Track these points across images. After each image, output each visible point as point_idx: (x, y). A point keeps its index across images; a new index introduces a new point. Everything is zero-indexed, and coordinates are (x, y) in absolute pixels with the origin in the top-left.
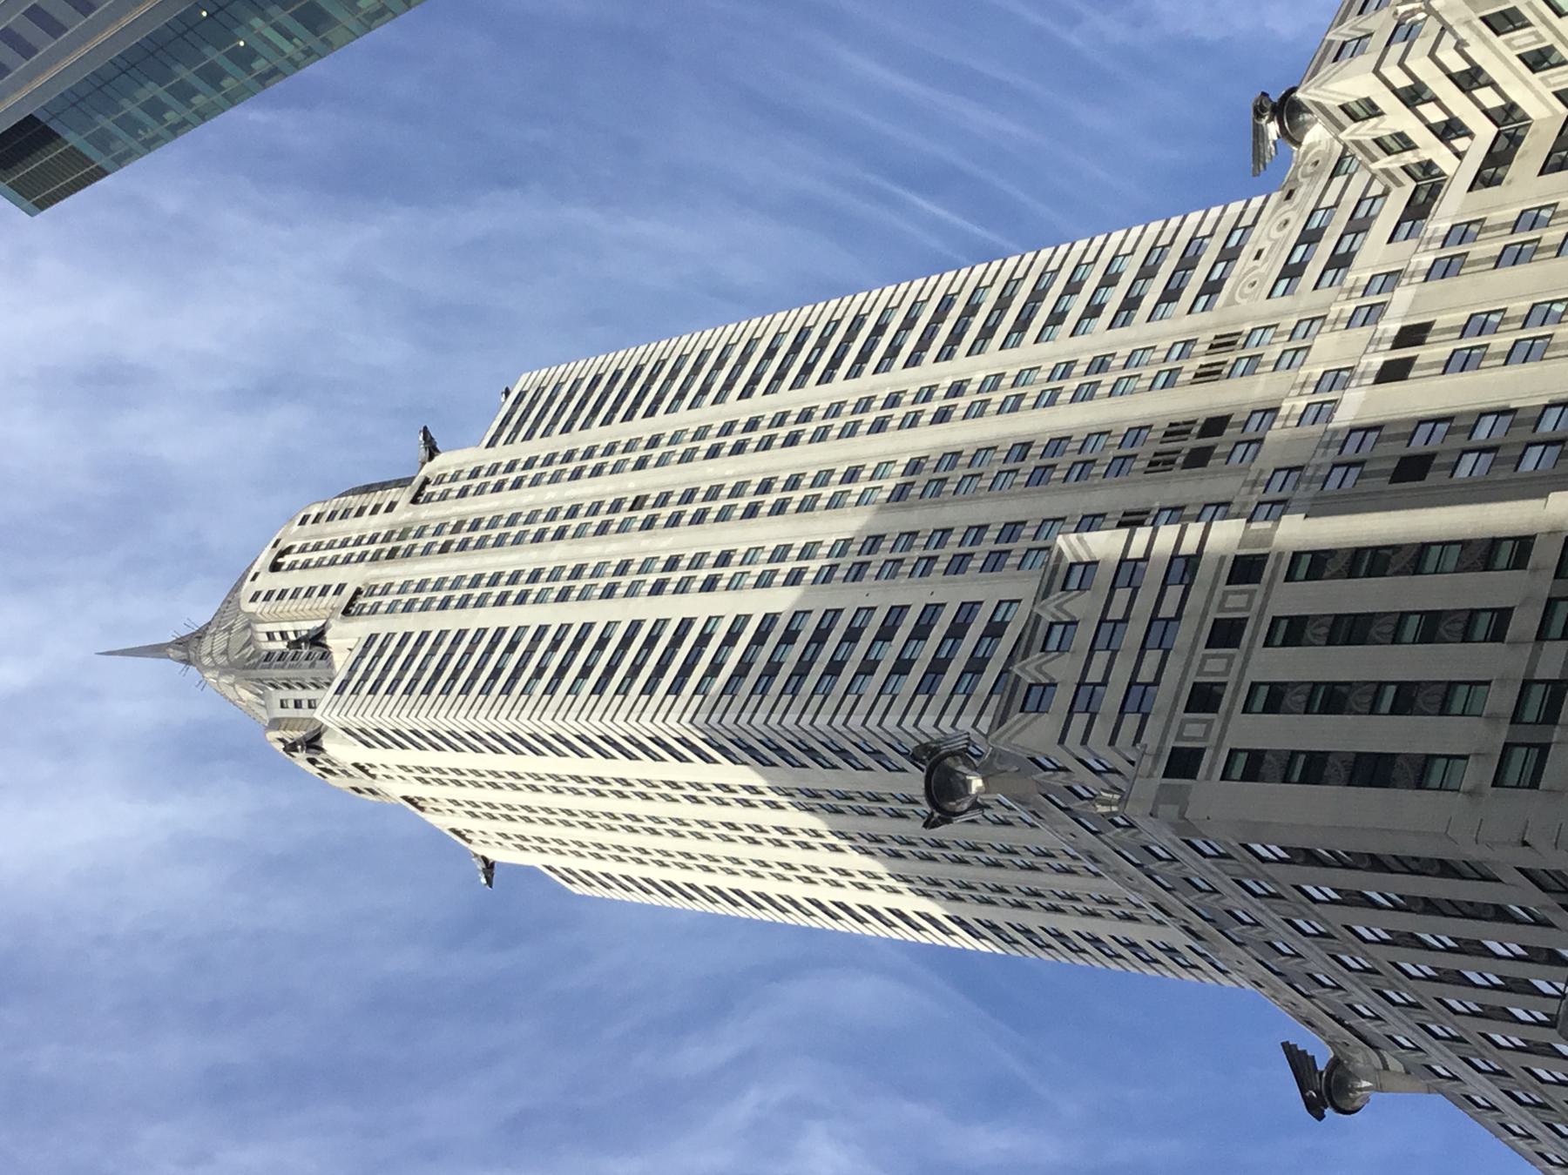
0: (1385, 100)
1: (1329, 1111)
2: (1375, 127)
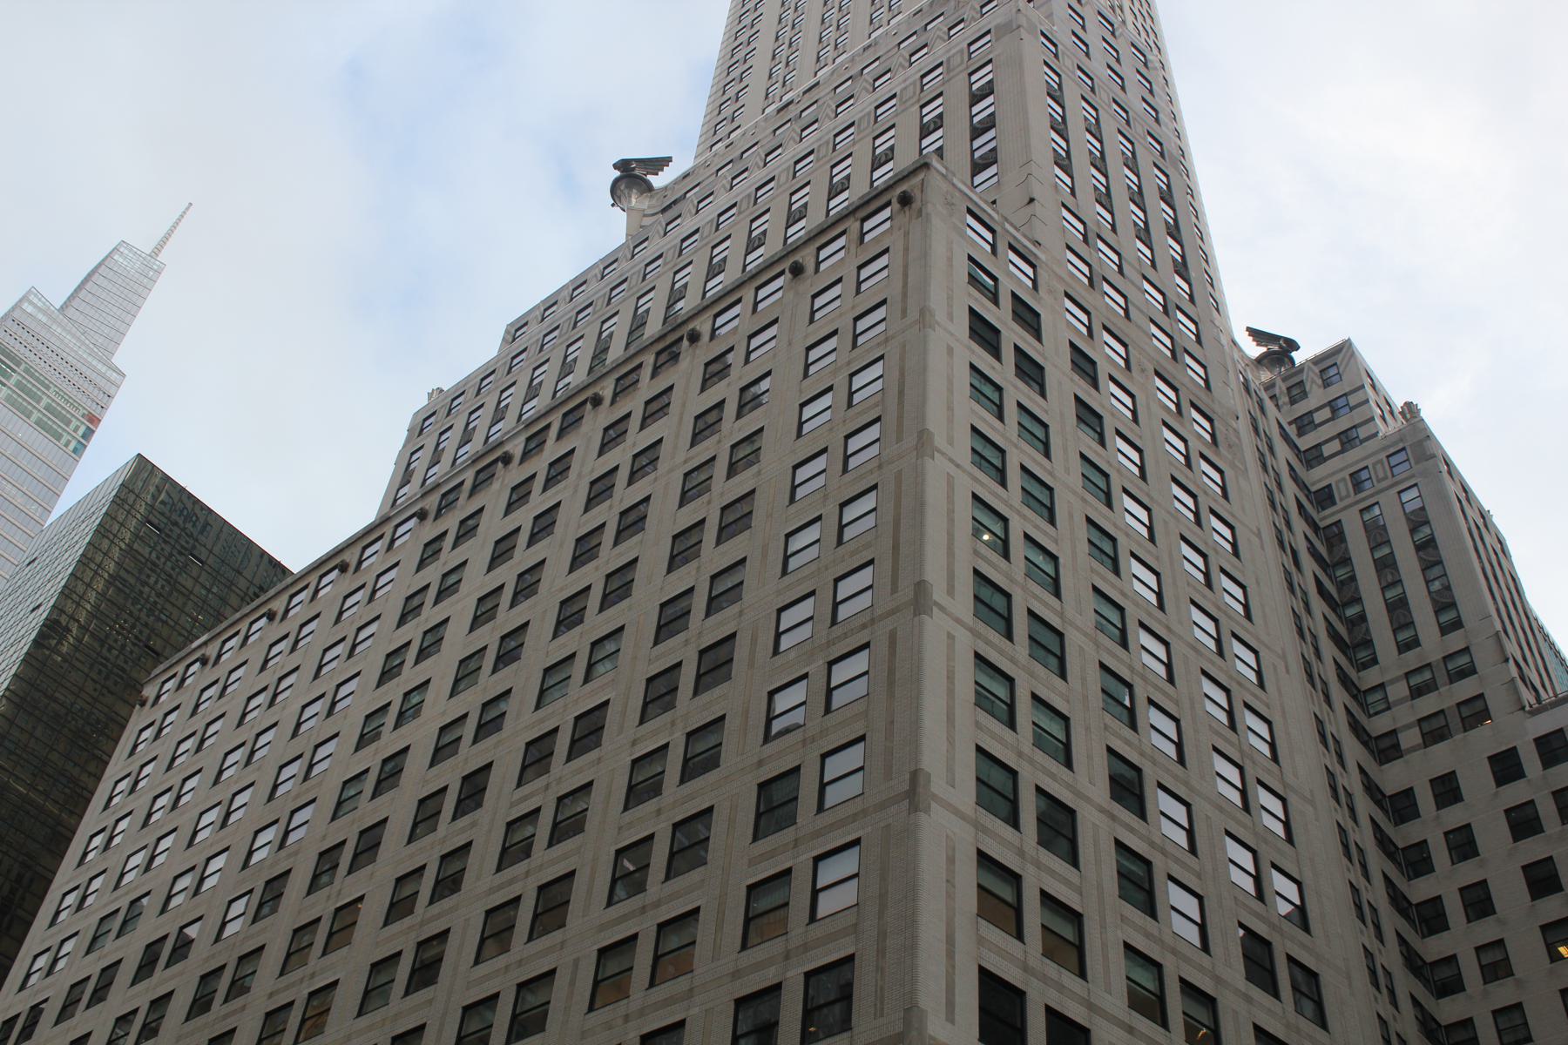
0: (1334, 391)
1: (617, 173)
2: (1313, 382)
